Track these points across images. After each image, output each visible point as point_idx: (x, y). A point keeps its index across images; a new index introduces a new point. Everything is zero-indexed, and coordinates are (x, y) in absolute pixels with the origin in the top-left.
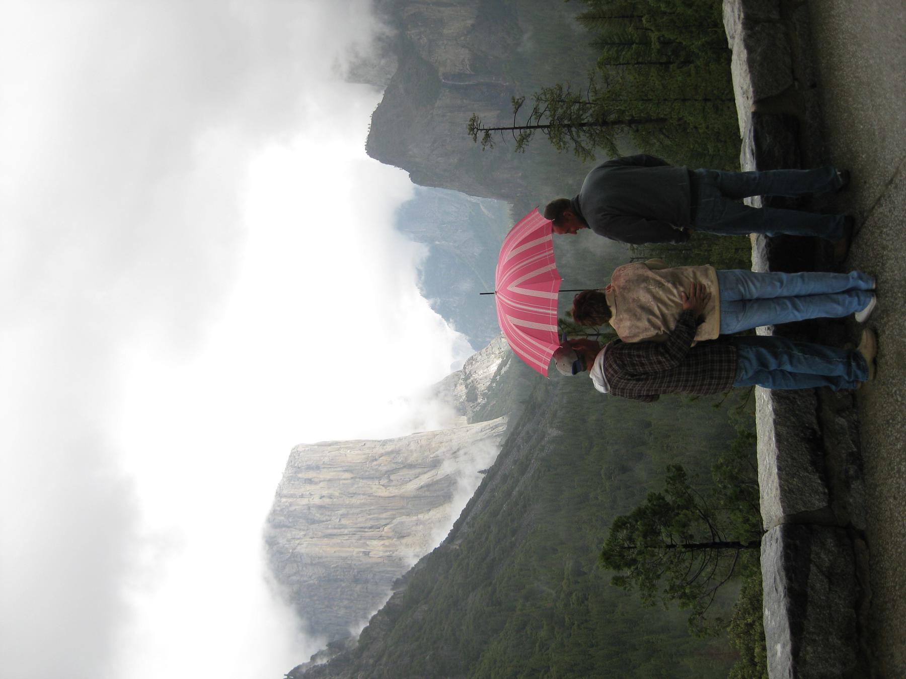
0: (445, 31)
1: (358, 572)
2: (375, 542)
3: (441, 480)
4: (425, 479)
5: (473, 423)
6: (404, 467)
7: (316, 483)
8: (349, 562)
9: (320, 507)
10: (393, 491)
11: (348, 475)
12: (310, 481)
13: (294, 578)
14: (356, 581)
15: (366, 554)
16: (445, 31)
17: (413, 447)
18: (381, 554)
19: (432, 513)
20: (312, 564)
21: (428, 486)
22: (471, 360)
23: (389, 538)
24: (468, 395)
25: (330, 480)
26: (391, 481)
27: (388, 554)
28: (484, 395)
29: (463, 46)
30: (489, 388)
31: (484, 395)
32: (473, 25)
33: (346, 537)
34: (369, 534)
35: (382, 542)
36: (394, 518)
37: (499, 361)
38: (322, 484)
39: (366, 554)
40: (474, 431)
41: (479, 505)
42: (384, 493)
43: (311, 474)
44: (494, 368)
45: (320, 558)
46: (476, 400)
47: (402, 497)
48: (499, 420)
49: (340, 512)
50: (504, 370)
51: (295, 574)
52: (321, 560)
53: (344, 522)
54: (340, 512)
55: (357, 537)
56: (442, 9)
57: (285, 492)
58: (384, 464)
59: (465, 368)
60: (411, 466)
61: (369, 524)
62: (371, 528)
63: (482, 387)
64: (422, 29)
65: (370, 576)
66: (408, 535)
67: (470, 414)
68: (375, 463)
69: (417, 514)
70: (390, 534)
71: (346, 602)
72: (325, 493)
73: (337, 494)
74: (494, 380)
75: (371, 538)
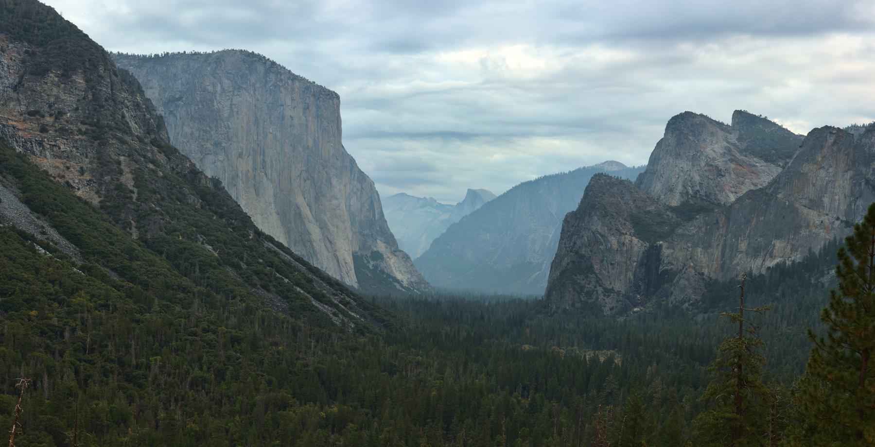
0: (699, 250)
1: (224, 147)
2: (251, 163)
3: (305, 226)
4: (306, 211)
5: (353, 255)
6: (317, 194)
7: (304, 113)
8: (234, 139)
11: (310, 142)
12: (306, 108)
13: (219, 88)
14: (217, 144)
15: (240, 155)
16: (699, 250)
18: (240, 169)
19: (275, 216)
20: (231, 105)
21: (299, 214)
22: (406, 258)
23: (255, 176)
24: (377, 252)
25: (307, 126)
26: (305, 181)
27: (240, 175)
28: (376, 267)
29: (685, 265)
30: (382, 272)
32: (703, 274)
33: (255, 138)
34: (259, 159)
35: (250, 170)
36: (271, 182)
38: (303, 118)
40: (346, 256)
41: (288, 258)
43: (313, 109)
44: (399, 276)
46: (373, 260)
48: (355, 279)
49: (278, 134)
50: (398, 286)
51: (222, 88)
52: (235, 114)
53: (270, 136)
54: (278, 134)
56: (720, 247)
59: (400, 251)
60: (317, 199)
61: (268, 160)
62: (264, 161)
63: (383, 265)
64: (703, 229)
65: (221, 158)
66: (257, 194)
67: (359, 254)
68: (321, 168)
69: (275, 202)
70: (257, 178)
71: (197, 134)
72: (296, 121)
73: (295, 132)
74: (389, 276)
75: (255, 161)
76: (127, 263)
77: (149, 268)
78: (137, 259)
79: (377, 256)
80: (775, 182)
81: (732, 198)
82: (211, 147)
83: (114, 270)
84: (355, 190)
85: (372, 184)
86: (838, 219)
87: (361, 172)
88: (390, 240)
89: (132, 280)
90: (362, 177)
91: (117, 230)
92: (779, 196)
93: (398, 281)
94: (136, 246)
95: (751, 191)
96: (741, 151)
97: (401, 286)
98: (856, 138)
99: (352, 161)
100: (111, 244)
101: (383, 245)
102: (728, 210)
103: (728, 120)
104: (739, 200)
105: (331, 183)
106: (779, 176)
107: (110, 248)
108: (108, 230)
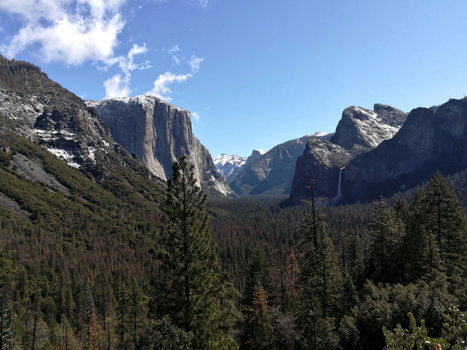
9: (165, 124)
10: (172, 153)
14: (135, 138)
15: (147, 142)
17: (190, 160)
18: (147, 148)
28: (212, 188)
30: (215, 190)
31: (212, 188)
37: (225, 194)
38: (174, 123)
39: (147, 142)
42: (172, 148)
44: (223, 192)
45: (144, 123)
46: (210, 185)
47: (170, 156)
53: (159, 132)
55: (153, 138)
57: (171, 108)
58: (183, 149)
61: (159, 143)
63: (215, 187)
65: (137, 143)
74: (217, 192)
76: (90, 194)
77: (101, 196)
78: (96, 192)
79: (212, 184)
80: (397, 136)
81: (377, 144)
82: (133, 139)
83: (84, 198)
84: (200, 154)
85: (207, 151)
86: (429, 150)
87: (202, 146)
88: (217, 176)
89: (93, 202)
90: (203, 148)
91: (86, 179)
92: (399, 142)
93: (222, 194)
94: (95, 186)
95: (385, 141)
96: (379, 122)
97: (224, 196)
98: (434, 112)
99: (198, 141)
100: (83, 186)
101: (214, 178)
102: (375, 150)
103: (372, 109)
104: (380, 145)
105: (188, 153)
106: (398, 133)
107: (83, 188)
108: (82, 179)
